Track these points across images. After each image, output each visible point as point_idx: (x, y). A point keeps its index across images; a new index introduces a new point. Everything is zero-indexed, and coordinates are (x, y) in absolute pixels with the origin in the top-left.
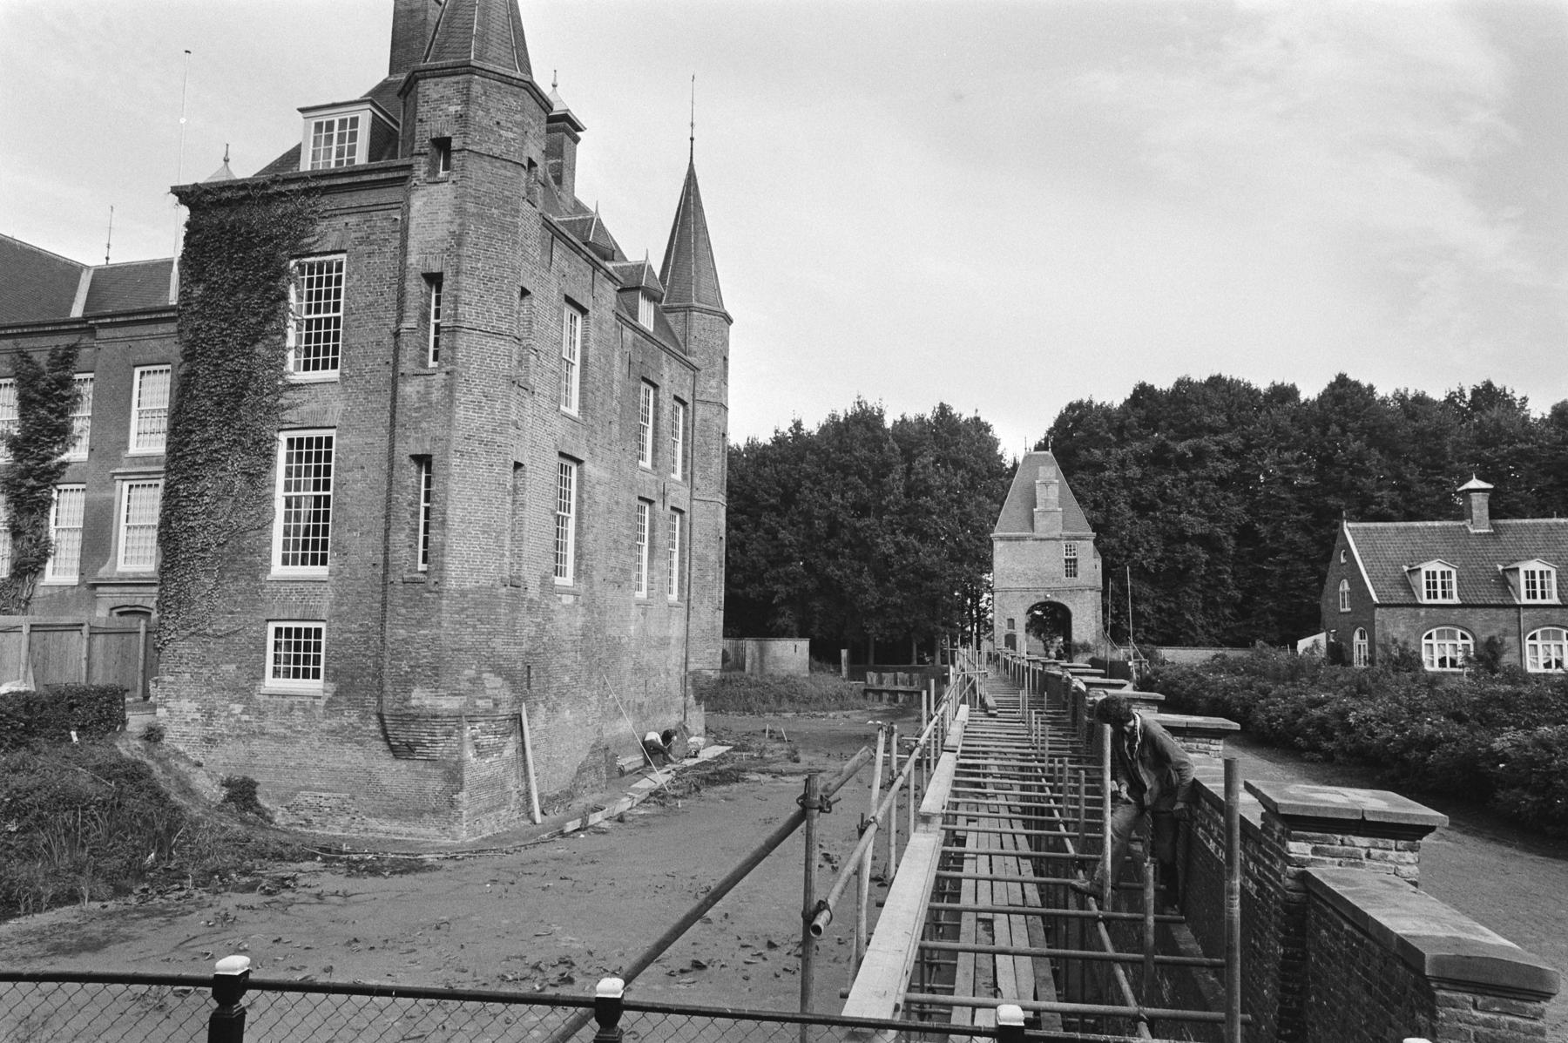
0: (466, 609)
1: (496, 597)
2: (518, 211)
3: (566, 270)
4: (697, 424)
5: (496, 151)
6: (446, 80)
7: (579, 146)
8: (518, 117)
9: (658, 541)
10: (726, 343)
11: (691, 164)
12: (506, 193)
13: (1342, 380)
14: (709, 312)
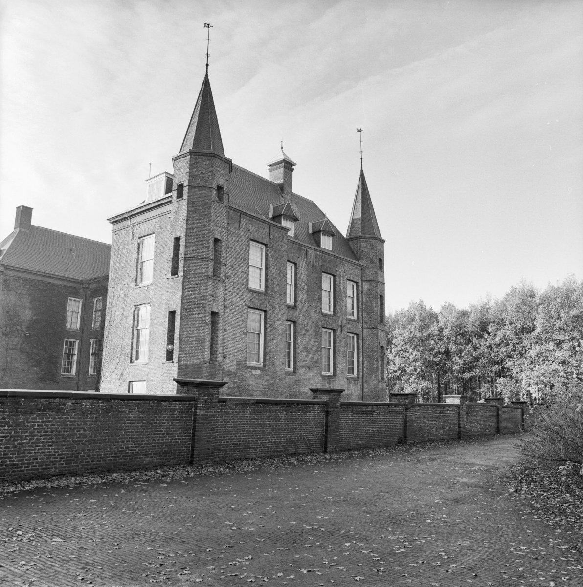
0: (188, 373)
1: (201, 368)
2: (211, 207)
3: (251, 228)
4: (365, 292)
5: (201, 184)
6: (182, 159)
7: (294, 172)
8: (211, 169)
9: (338, 348)
10: (382, 252)
11: (362, 170)
12: (206, 200)
13: (31, 209)
14: (369, 238)
